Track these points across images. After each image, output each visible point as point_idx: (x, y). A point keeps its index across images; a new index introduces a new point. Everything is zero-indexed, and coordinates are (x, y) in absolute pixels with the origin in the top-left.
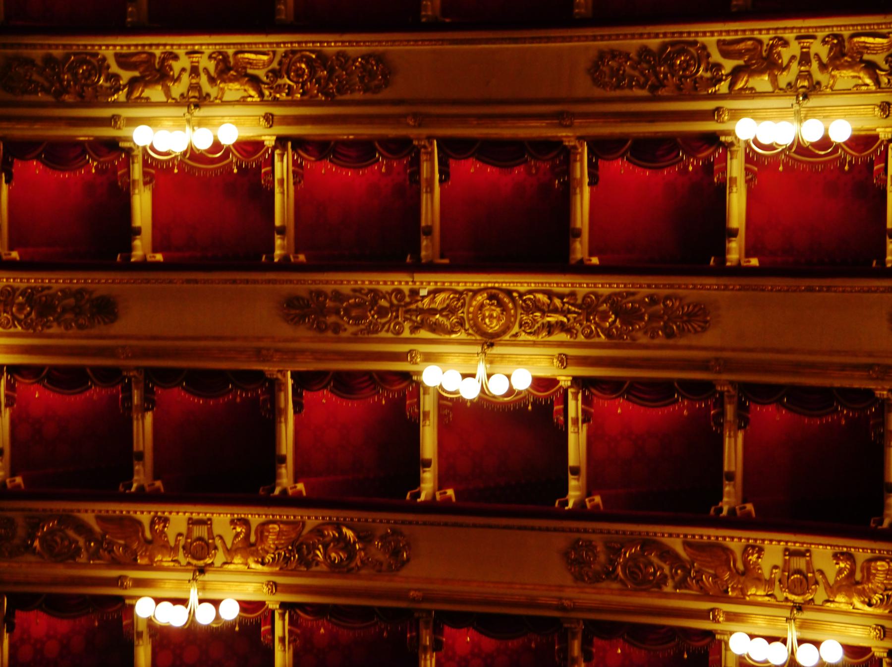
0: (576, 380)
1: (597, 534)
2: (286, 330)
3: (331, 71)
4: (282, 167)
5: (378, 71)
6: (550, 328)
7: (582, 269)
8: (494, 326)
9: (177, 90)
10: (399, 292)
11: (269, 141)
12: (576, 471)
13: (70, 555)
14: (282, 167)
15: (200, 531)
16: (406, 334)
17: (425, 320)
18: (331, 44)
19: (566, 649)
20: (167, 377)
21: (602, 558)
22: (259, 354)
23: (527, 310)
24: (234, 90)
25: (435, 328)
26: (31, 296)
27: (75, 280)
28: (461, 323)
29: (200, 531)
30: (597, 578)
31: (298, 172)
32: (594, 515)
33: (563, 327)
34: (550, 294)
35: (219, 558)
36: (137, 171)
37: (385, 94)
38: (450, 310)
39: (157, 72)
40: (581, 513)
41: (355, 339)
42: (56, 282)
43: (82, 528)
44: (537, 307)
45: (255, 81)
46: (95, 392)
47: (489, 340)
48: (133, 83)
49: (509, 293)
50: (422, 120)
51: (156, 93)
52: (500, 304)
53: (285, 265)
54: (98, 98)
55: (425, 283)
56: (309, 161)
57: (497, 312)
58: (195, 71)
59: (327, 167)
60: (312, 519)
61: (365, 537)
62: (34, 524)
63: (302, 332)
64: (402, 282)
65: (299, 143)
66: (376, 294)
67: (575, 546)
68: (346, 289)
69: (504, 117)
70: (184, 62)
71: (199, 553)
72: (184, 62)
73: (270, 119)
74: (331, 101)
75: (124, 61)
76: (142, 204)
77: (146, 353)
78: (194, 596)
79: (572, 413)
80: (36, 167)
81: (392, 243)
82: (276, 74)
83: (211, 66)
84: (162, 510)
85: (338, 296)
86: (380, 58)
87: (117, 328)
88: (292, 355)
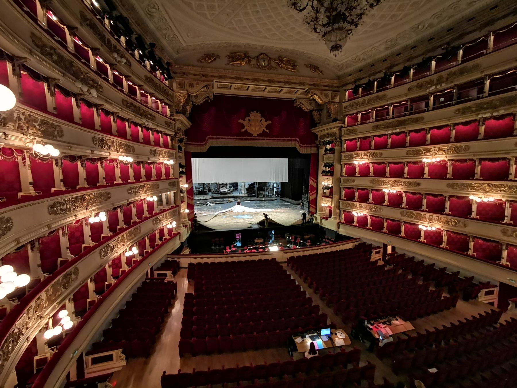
0: (507, 200)
1: (510, 228)
2: (447, 188)
3: (458, 149)
4: (449, 164)
5: (467, 148)
6: (501, 191)
7: (511, 180)
8: (488, 190)
9: (431, 153)
10: (468, 184)
11: (447, 160)
12: (507, 216)
13: (412, 217)
14: (449, 164)
15: (431, 217)
16: (469, 190)
17: (473, 188)
18: (458, 144)
19: (502, 247)
20: (429, 194)
21: (510, 232)
22: (442, 192)
23: (495, 187)
24: (441, 152)
25: (476, 189)
26: (408, 182)
27: (415, 180)
28: (481, 189)
29: (431, 217)
30: (508, 236)
31: (452, 164)
32: (510, 224)
33: (504, 191)
34: (501, 185)
35: (434, 221)
36: (426, 165)
37: (468, 152)
38: (478, 187)
39: (429, 151)
40: (506, 224)
41: (459, 190)
42: (411, 180)
43: (413, 214)
44: (498, 187)
45: (445, 151)
46: (418, 196)
47: (487, 192)
48: (425, 153)
49: (492, 184)
50: (474, 155)
51: (428, 154)
52: (489, 186)
53: (448, 179)
54: (420, 155)
55: (473, 182)
56: (454, 162)
57: (488, 187)
58: (435, 150)
59: (458, 163)
60: (450, 217)
61: (459, 222)
62: (407, 212)
63: (450, 189)
64: (470, 182)
65: (452, 160)
66: (464, 184)
67: (504, 229)
68: (458, 183)
69: (498, 154)
70: (433, 149)
71: (431, 220)
72: (433, 149)
73: (446, 157)
74: (458, 153)
75: (424, 150)
76: (426, 170)
77: (425, 191)
78: (428, 226)
79: (507, 206)
80: (412, 165)
81: (469, 175)
82: (448, 150)
83: (438, 149)
84: (425, 213)
85: (457, 184)
86: (467, 146)
87: (420, 187)
88: (447, 192)
